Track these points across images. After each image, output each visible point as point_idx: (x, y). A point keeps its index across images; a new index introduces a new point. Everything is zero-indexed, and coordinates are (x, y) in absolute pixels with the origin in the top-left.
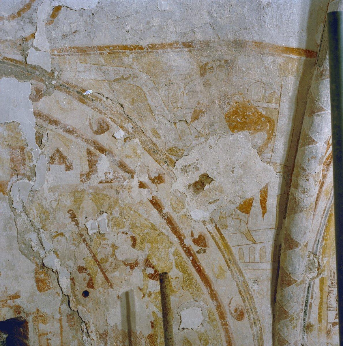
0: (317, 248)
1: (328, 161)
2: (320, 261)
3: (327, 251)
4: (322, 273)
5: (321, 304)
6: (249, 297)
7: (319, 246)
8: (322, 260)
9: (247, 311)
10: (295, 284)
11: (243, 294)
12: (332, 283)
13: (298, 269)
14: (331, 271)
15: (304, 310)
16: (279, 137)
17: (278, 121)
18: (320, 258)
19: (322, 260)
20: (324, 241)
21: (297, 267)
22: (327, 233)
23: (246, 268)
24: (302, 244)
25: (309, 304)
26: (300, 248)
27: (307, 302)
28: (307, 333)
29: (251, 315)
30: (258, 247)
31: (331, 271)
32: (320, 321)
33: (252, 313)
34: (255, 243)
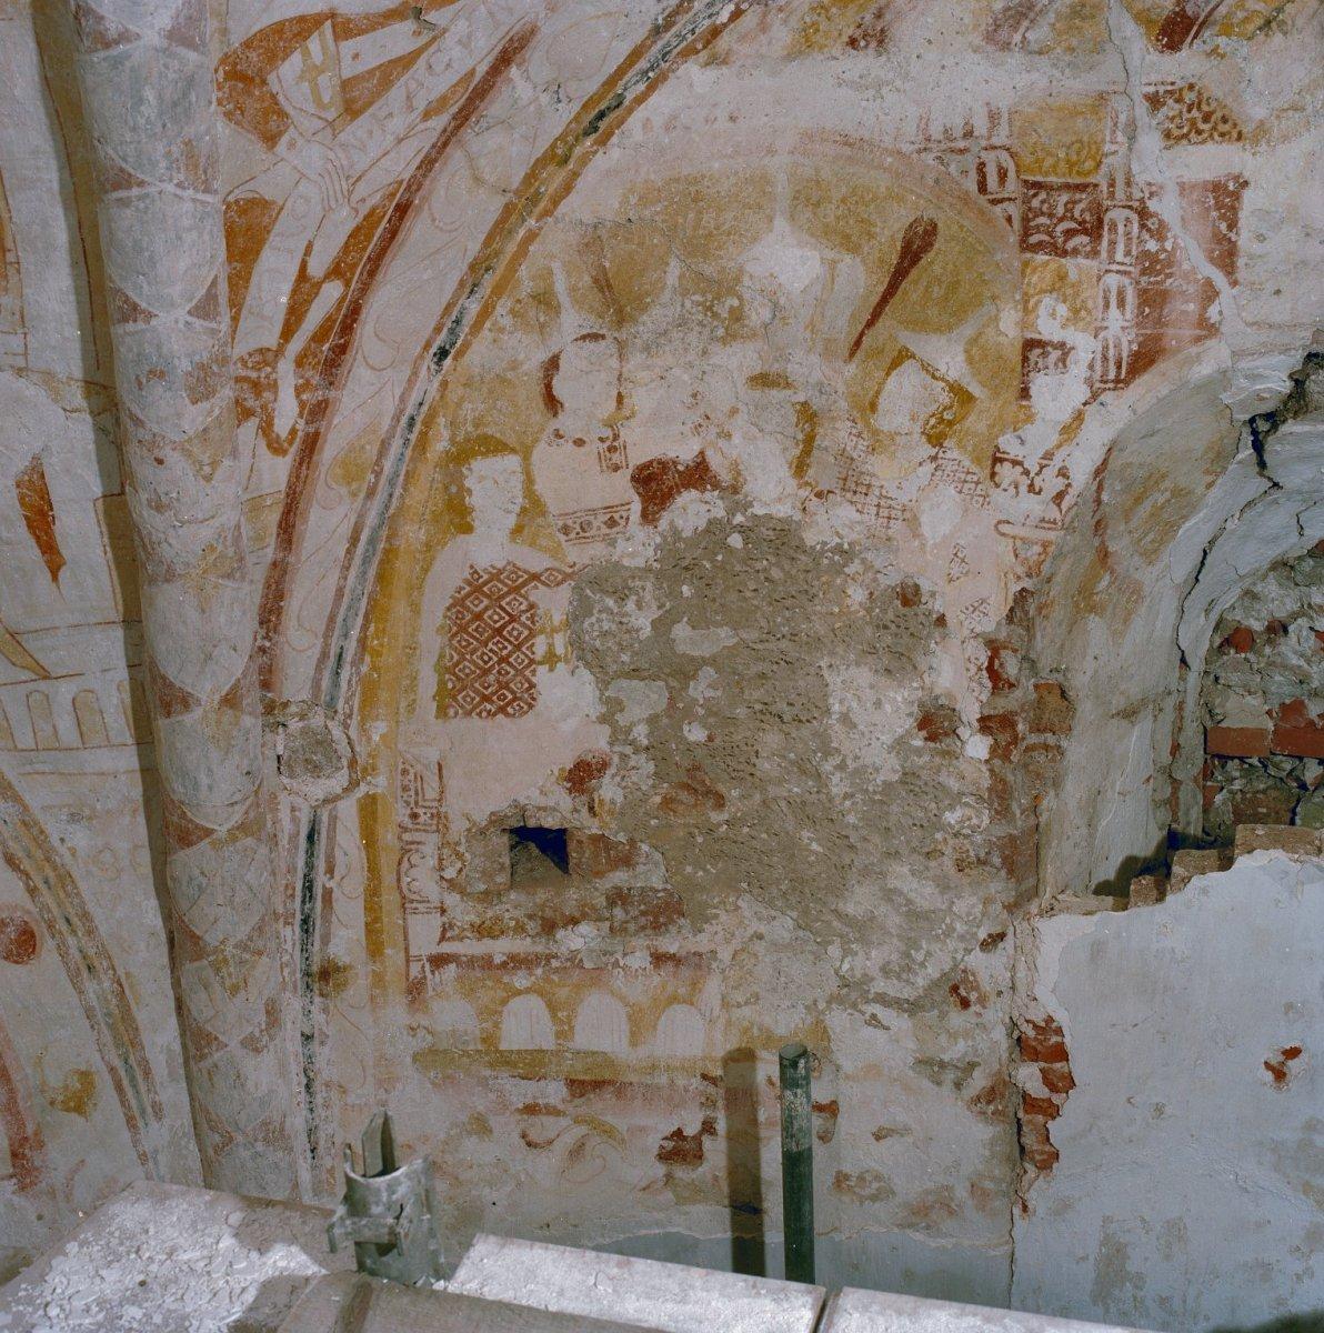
0: (336, 685)
1: (326, 347)
2: (353, 733)
3: (384, 695)
4: (364, 778)
5: (372, 893)
6: (51, 874)
7: (345, 674)
8: (363, 729)
9: (50, 926)
10: (208, 840)
11: (26, 865)
12: (414, 816)
13: (210, 788)
14: (405, 772)
15: (299, 917)
16: (32, 268)
17: (10, 201)
18: (354, 723)
19: (363, 729)
20: (367, 658)
21: (204, 780)
22: (377, 629)
23: (28, 768)
24: (203, 697)
25: (318, 891)
26: (197, 713)
27: (309, 887)
28: (322, 995)
29: (71, 941)
30: (65, 692)
31: (405, 772)
32: (375, 949)
33: (74, 932)
34: (47, 677)
